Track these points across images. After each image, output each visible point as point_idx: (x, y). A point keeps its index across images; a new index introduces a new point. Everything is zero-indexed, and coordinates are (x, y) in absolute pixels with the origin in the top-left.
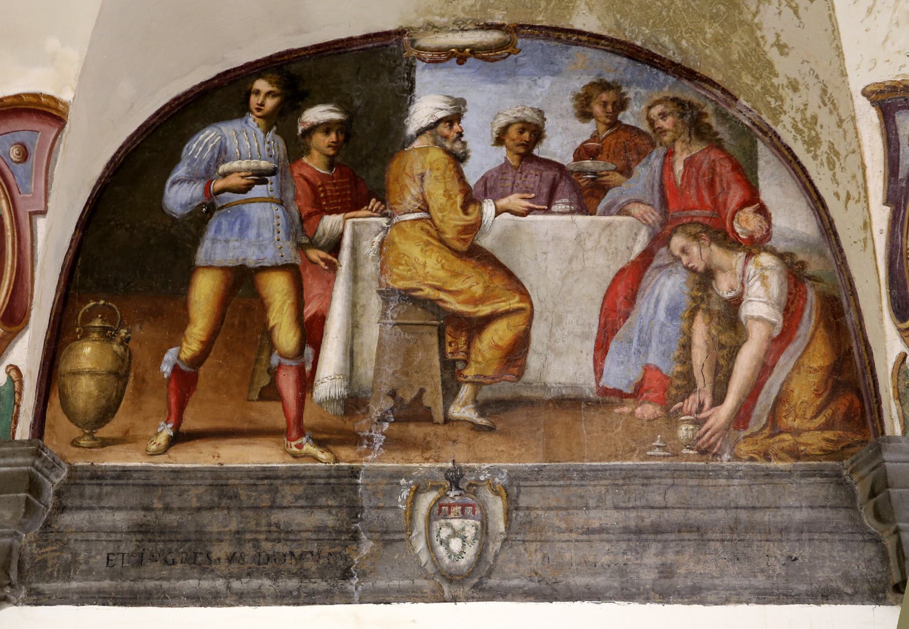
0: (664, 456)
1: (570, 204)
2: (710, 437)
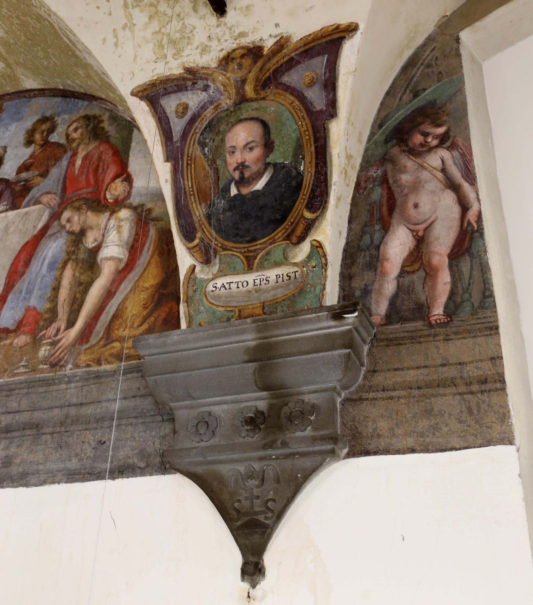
0: (25, 373)
1: (7, 205)
2: (61, 353)
